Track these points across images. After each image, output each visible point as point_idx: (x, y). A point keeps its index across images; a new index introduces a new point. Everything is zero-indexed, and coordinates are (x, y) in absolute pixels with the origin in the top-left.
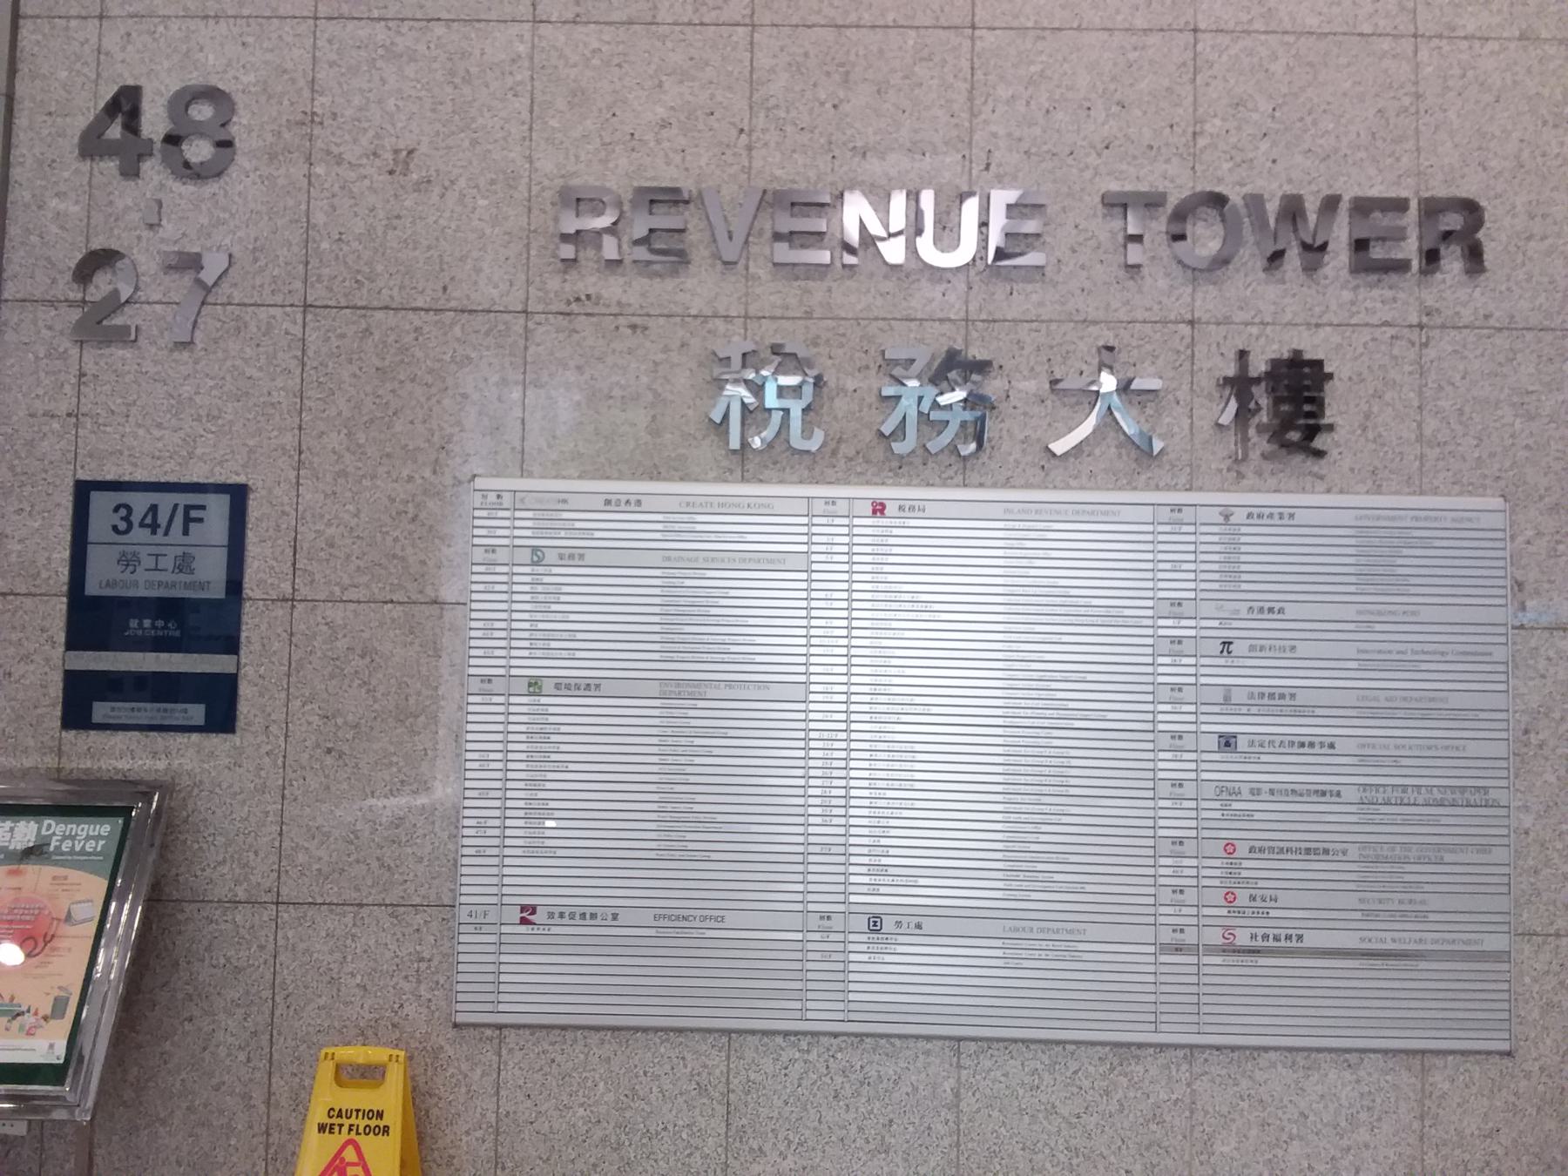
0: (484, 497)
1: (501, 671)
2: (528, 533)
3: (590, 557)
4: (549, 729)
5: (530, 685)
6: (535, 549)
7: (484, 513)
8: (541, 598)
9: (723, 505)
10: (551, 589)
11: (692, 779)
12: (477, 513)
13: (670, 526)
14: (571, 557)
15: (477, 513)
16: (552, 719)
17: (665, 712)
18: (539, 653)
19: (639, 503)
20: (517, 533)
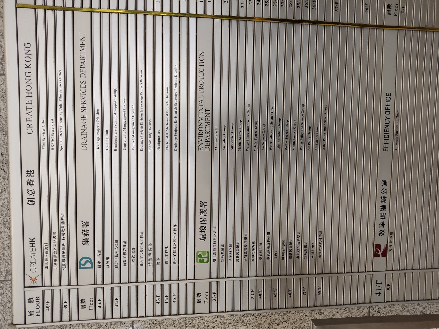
0: (31, 314)
2: (64, 272)
5: (202, 261)
6: (78, 266)
7: (48, 313)
8: (125, 257)
9: (29, 93)
13: (52, 144)
14: (85, 233)
18: (174, 256)
19: (30, 173)
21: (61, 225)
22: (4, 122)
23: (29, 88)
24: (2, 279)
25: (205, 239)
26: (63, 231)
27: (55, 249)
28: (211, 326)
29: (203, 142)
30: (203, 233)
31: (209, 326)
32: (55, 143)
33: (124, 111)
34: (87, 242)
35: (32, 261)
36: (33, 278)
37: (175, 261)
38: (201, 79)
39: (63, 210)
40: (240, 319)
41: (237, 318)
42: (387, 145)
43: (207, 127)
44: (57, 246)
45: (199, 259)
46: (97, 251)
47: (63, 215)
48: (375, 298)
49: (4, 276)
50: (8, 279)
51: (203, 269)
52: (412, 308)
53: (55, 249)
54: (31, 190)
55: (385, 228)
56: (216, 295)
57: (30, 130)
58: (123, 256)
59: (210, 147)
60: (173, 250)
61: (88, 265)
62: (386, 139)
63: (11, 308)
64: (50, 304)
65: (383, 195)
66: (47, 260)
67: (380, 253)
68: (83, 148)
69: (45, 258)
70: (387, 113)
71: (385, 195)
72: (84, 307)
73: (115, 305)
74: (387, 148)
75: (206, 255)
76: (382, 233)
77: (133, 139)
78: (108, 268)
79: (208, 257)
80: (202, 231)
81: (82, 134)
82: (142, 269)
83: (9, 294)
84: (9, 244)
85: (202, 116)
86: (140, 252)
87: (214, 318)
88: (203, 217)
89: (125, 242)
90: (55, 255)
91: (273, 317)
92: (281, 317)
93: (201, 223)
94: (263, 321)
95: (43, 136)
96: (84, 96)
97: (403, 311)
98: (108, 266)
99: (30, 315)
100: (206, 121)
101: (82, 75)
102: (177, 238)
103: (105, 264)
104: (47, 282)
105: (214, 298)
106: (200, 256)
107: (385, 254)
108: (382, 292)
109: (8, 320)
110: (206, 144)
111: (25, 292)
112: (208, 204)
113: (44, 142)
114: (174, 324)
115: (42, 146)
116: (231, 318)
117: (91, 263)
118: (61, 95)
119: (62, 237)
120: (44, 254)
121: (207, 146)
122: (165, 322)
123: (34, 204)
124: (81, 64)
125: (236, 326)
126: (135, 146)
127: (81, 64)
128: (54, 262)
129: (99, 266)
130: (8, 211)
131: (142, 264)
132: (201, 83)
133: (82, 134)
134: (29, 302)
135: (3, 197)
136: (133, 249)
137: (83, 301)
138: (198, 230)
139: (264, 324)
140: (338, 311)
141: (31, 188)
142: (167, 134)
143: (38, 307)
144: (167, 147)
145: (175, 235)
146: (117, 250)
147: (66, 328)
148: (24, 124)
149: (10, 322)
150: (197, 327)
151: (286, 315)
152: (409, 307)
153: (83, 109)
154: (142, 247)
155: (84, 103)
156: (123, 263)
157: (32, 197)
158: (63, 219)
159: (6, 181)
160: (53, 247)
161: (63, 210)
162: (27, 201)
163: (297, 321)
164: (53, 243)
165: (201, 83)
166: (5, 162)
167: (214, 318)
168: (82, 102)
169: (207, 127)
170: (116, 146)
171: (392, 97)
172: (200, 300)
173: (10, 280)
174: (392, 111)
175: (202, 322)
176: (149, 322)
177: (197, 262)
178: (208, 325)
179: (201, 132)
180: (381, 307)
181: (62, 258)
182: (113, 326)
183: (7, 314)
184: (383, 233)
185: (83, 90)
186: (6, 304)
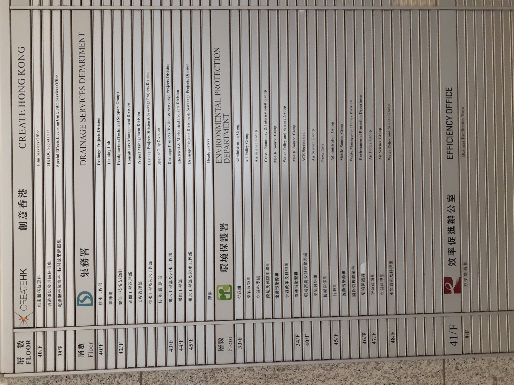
0: (21, 360)
2: (60, 311)
3: (84, 241)
5: (223, 298)
6: (77, 302)
7: (40, 361)
8: (130, 292)
10: (120, 282)
11: (313, 126)
12: (40, 367)
13: (48, 158)
14: (84, 262)
15: (40, 367)
17: (247, 156)
18: (190, 291)
19: (22, 193)
20: (60, 322)
21: (57, 253)
23: (22, 97)
25: (227, 270)
26: (59, 260)
28: (237, 382)
29: (222, 153)
30: (224, 263)
31: (235, 381)
32: (51, 157)
33: (128, 119)
36: (24, 317)
37: (190, 297)
38: (217, 80)
39: (59, 236)
40: (274, 374)
41: (270, 372)
43: (226, 136)
44: (52, 277)
45: (220, 295)
46: (98, 285)
47: (59, 242)
48: (450, 349)
51: (224, 308)
52: (501, 364)
54: (23, 213)
55: (456, 256)
57: (22, 144)
59: (230, 158)
60: (188, 284)
61: (88, 301)
62: (450, 143)
64: (42, 350)
65: (450, 214)
66: (39, 296)
67: (452, 289)
68: (82, 162)
69: (38, 293)
70: (448, 111)
71: (453, 214)
72: (82, 353)
73: (119, 351)
74: (451, 155)
75: (229, 291)
76: (452, 262)
77: (139, 152)
79: (230, 293)
80: (222, 261)
81: (81, 146)
82: (151, 307)
85: (219, 122)
86: (148, 287)
87: (242, 371)
88: (223, 242)
89: (130, 274)
90: (49, 288)
91: (316, 372)
92: (326, 372)
93: (221, 250)
94: (304, 377)
95: (38, 150)
96: (83, 103)
97: (490, 368)
98: (110, 302)
100: (225, 128)
101: (82, 81)
103: (108, 300)
104: (40, 323)
105: (240, 345)
106: (221, 291)
107: (458, 290)
108: (459, 340)
111: (14, 333)
113: (38, 157)
114: (191, 377)
115: (36, 162)
118: (57, 104)
119: (57, 267)
121: (226, 158)
122: (181, 375)
123: (26, 229)
125: (269, 382)
128: (48, 298)
129: (100, 303)
131: (151, 301)
132: (217, 83)
133: (81, 146)
134: (18, 346)
138: (218, 259)
139: (305, 380)
140: (402, 366)
141: (24, 210)
142: (179, 144)
143: (28, 353)
144: (180, 160)
145: (190, 265)
146: (121, 283)
147: (61, 380)
150: (220, 382)
151: (333, 370)
152: (498, 362)
154: (150, 280)
156: (128, 299)
157: (24, 220)
160: (47, 279)
161: (59, 236)
163: (347, 377)
165: (217, 83)
167: (242, 371)
168: (81, 111)
169: (226, 136)
170: (119, 159)
171: (454, 92)
172: (222, 347)
174: (454, 109)
175: (226, 376)
176: (161, 375)
177: (218, 299)
178: (233, 380)
179: (219, 141)
180: (460, 362)
182: (117, 379)
184: (453, 262)
185: (83, 97)
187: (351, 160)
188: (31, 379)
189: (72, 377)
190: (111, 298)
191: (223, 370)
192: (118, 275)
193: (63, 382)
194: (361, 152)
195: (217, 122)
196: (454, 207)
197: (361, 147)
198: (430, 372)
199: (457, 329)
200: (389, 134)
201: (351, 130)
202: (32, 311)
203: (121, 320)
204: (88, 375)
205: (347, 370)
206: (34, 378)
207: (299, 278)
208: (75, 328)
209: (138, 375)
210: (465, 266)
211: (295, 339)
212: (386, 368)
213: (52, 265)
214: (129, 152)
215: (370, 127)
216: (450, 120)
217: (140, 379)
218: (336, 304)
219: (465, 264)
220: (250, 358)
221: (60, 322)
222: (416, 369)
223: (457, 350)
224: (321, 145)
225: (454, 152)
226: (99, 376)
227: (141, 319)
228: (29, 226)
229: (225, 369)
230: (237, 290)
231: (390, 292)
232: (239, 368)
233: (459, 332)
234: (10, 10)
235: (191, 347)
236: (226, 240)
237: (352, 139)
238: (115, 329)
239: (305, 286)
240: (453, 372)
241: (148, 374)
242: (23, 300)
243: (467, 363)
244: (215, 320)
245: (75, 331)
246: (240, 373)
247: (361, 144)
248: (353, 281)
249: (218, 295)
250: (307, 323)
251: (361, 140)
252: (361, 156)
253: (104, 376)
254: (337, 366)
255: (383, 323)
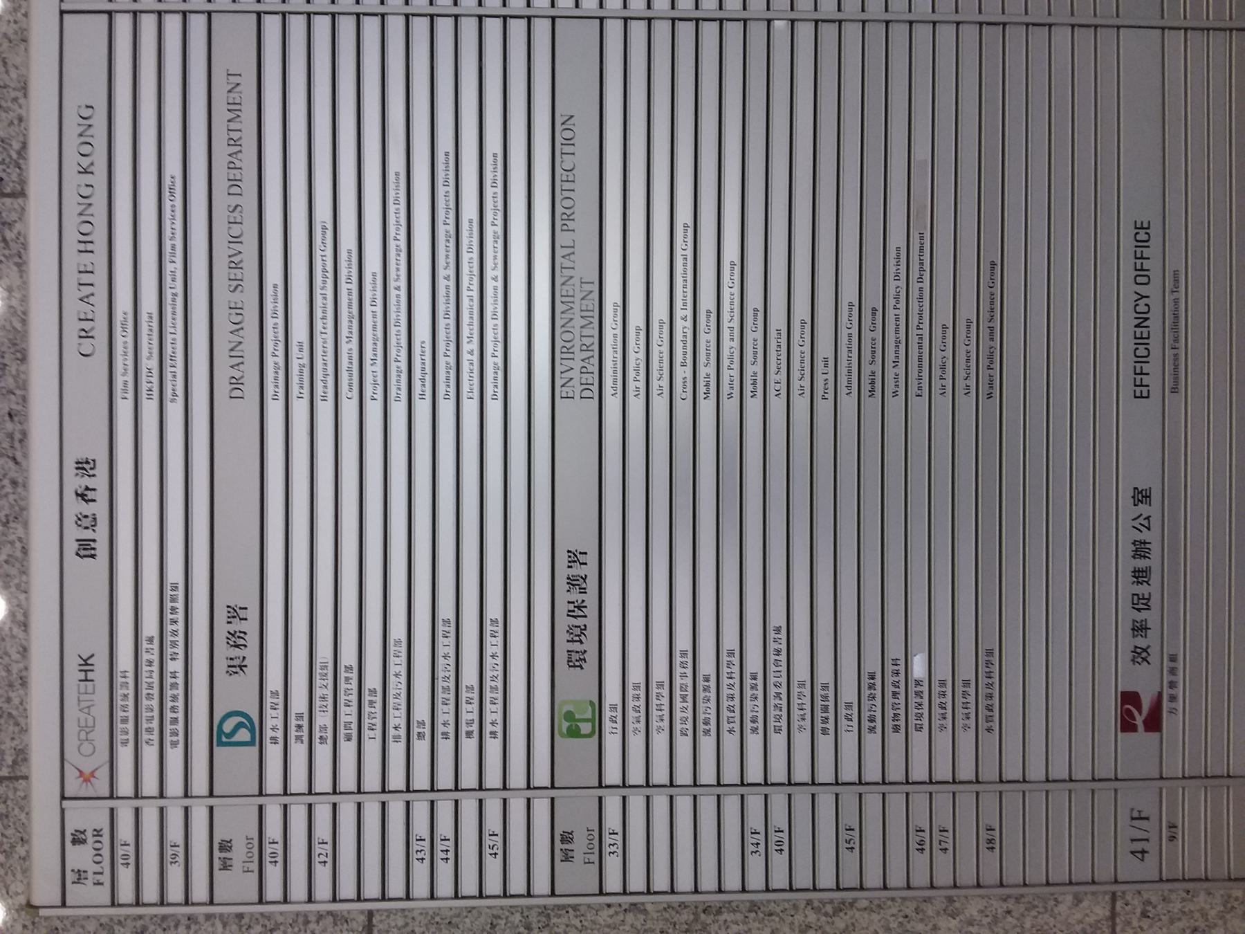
0: (80, 875)
1: (541, 808)
2: (174, 757)
3: (237, 587)
4: (683, 680)
5: (574, 733)
6: (217, 738)
8: (348, 714)
9: (85, 241)
10: (323, 689)
11: (801, 310)
12: (126, 893)
13: (149, 382)
14: (236, 640)
15: (126, 893)
16: (660, 672)
18: (493, 714)
19: (84, 466)
20: (174, 785)
21: (170, 616)
22: (18, 326)
23: (86, 228)
24: (5, 772)
26: (174, 633)
27: (150, 686)
30: (576, 646)
32: (155, 380)
33: (348, 288)
34: (241, 667)
35: (83, 724)
36: (87, 771)
38: (566, 194)
39: (175, 573)
40: (696, 920)
41: (686, 916)
42: (1146, 380)
43: (586, 332)
44: (156, 676)
48: (1131, 868)
49: (10, 763)
50: (19, 774)
53: (150, 686)
54: (86, 517)
55: (1151, 640)
56: (619, 838)
57: (86, 346)
58: (343, 710)
59: (596, 388)
60: (488, 695)
61: (243, 735)
62: (1141, 360)
63: (26, 858)
64: (131, 850)
66: (125, 720)
67: (1139, 720)
70: (1139, 280)
71: (1145, 535)
74: (1145, 389)
76: (1140, 655)
77: (373, 370)
78: (299, 744)
79: (592, 720)
80: (573, 641)
83: (23, 816)
84: (24, 674)
86: (391, 701)
87: (617, 913)
88: (576, 596)
90: (149, 703)
91: (799, 918)
92: (823, 918)
93: (570, 614)
95: (123, 361)
97: (1228, 916)
98: (299, 738)
99: (78, 881)
102: (500, 661)
104: (125, 786)
105: (613, 849)
106: (569, 716)
107: (1154, 723)
108: (1151, 847)
109: (17, 894)
110: (584, 381)
111: (63, 811)
112: (592, 559)
116: (668, 916)
117: (252, 731)
118: (173, 247)
120: (119, 702)
121: (586, 387)
123: (93, 556)
124: (231, 159)
126: (380, 390)
127: (231, 159)
130: (24, 578)
131: (399, 737)
132: (568, 203)
133: (233, 354)
135: (12, 537)
136: (373, 692)
137: (226, 846)
138: (562, 636)
140: (1011, 907)
143: (98, 859)
146: (325, 691)
147: (176, 926)
148: (72, 327)
149: (22, 900)
151: (842, 914)
153: (235, 283)
155: (237, 266)
157: (88, 534)
158: (173, 600)
159: (19, 490)
160: (145, 680)
161: (175, 573)
162: (76, 545)
164: (145, 668)
165: (568, 203)
166: (18, 436)
167: (617, 913)
169: (586, 332)
170: (324, 387)
171: (1155, 231)
173: (26, 778)
174: (1155, 274)
175: (579, 925)
176: (419, 918)
177: (562, 735)
180: (1154, 899)
181: (169, 715)
182: (312, 926)
183: (14, 875)
184: (1144, 655)
185: (236, 230)
186: (13, 847)
187: (895, 394)
188: (103, 921)
189: (201, 919)
190: (299, 727)
191: (570, 910)
192: (319, 671)
193: (182, 929)
194: (920, 378)
195: (564, 299)
196: (1148, 518)
197: (920, 366)
198: (1080, 922)
199: (1147, 819)
200: (992, 334)
201: (897, 319)
202: (107, 758)
203: (323, 782)
204: (240, 916)
205: (875, 917)
206: (111, 920)
207: (761, 687)
208: (212, 801)
209: (362, 918)
210: (1172, 665)
211: (750, 840)
212: (972, 910)
213: (156, 645)
214: (349, 369)
215: (943, 315)
216: (1144, 301)
217: (369, 926)
218: (854, 753)
219: (1173, 658)
220: (637, 883)
221: (174, 785)
222: (1046, 916)
223: (1148, 869)
224: (821, 359)
225: (1153, 381)
226: (269, 918)
227: (372, 781)
228: (102, 548)
229: (575, 908)
230: (607, 713)
231: (986, 725)
232: (609, 906)
233: (1151, 825)
234: (62, 12)
235: (495, 851)
236: (583, 591)
237: (898, 342)
238: (310, 805)
239: (776, 706)
240: (1135, 923)
241: (388, 917)
242: (87, 729)
243: (1170, 901)
244: (553, 787)
245: (211, 809)
246: (611, 916)
247: (920, 359)
248: (895, 694)
249: (560, 726)
250: (778, 800)
251: (920, 348)
252: (920, 388)
253: (280, 919)
254: (852, 905)
255: (966, 800)
